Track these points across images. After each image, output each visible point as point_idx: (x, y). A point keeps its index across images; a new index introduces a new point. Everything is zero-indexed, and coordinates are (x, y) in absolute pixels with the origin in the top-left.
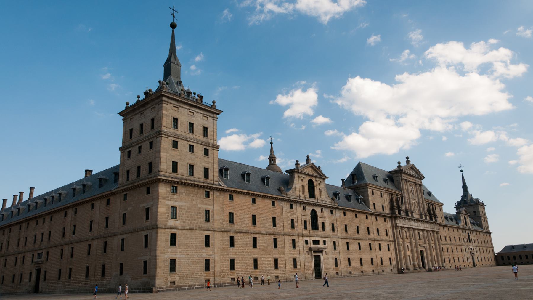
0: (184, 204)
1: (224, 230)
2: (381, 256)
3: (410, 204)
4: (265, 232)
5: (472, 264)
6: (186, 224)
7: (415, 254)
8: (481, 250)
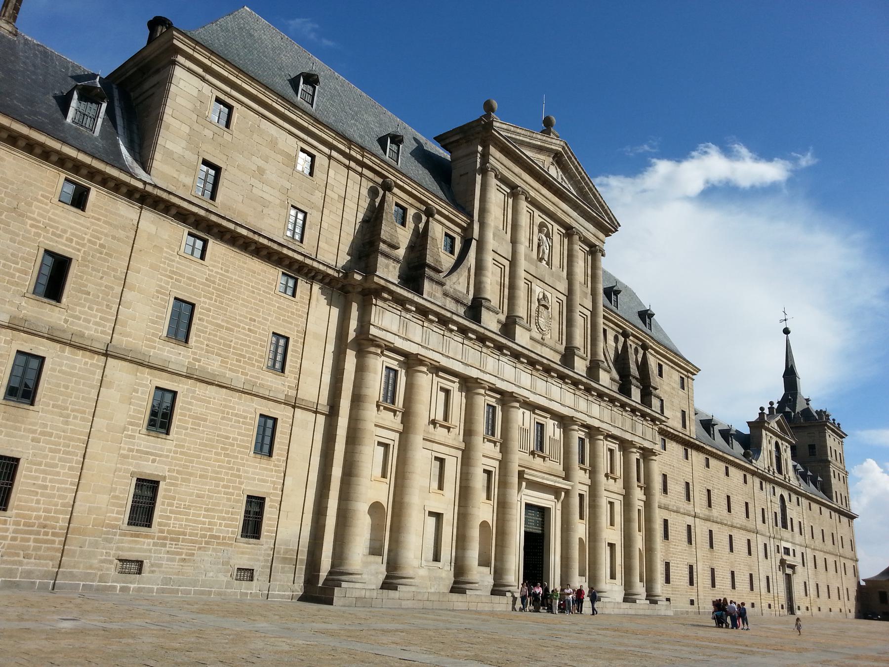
2: (150, 470)
3: (512, 287)
5: (783, 600)
7: (484, 511)
8: (821, 563)
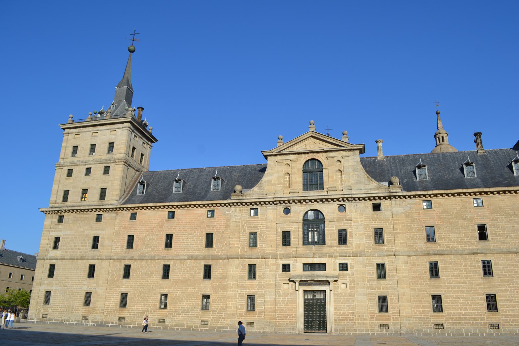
0: (68, 233)
1: (115, 257)
4: (186, 257)
6: (68, 254)
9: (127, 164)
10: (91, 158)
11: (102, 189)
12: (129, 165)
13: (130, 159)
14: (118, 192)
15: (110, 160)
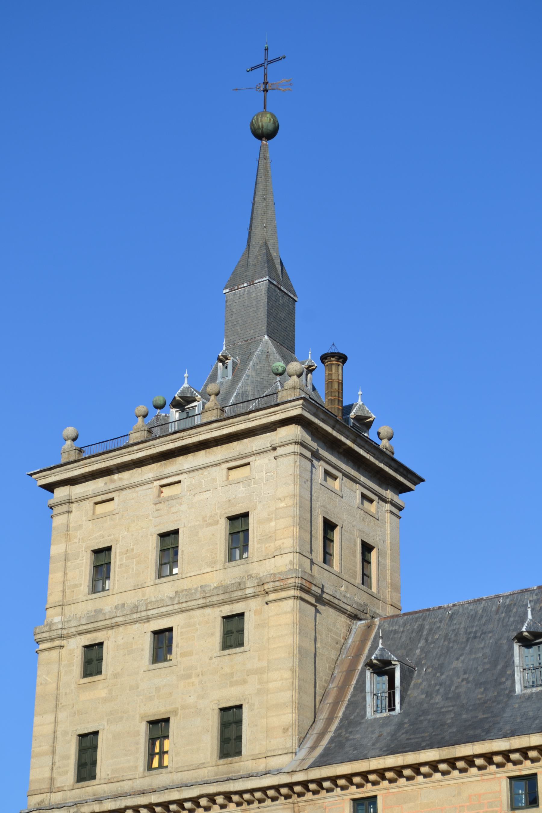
9: (313, 596)
10: (167, 588)
11: (223, 710)
12: (320, 599)
13: (320, 575)
14: (288, 717)
15: (240, 586)
